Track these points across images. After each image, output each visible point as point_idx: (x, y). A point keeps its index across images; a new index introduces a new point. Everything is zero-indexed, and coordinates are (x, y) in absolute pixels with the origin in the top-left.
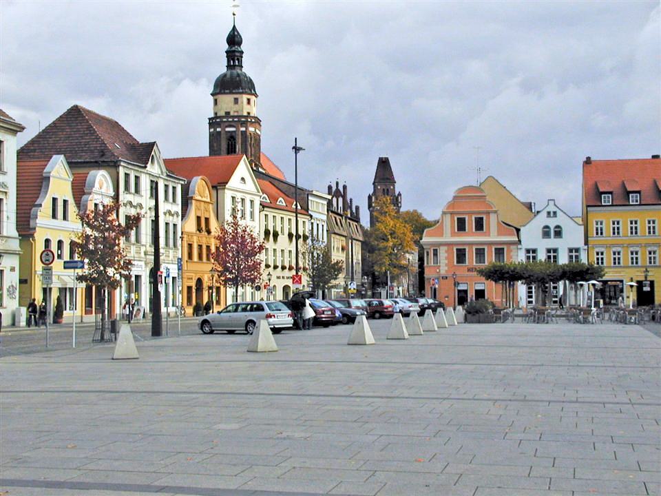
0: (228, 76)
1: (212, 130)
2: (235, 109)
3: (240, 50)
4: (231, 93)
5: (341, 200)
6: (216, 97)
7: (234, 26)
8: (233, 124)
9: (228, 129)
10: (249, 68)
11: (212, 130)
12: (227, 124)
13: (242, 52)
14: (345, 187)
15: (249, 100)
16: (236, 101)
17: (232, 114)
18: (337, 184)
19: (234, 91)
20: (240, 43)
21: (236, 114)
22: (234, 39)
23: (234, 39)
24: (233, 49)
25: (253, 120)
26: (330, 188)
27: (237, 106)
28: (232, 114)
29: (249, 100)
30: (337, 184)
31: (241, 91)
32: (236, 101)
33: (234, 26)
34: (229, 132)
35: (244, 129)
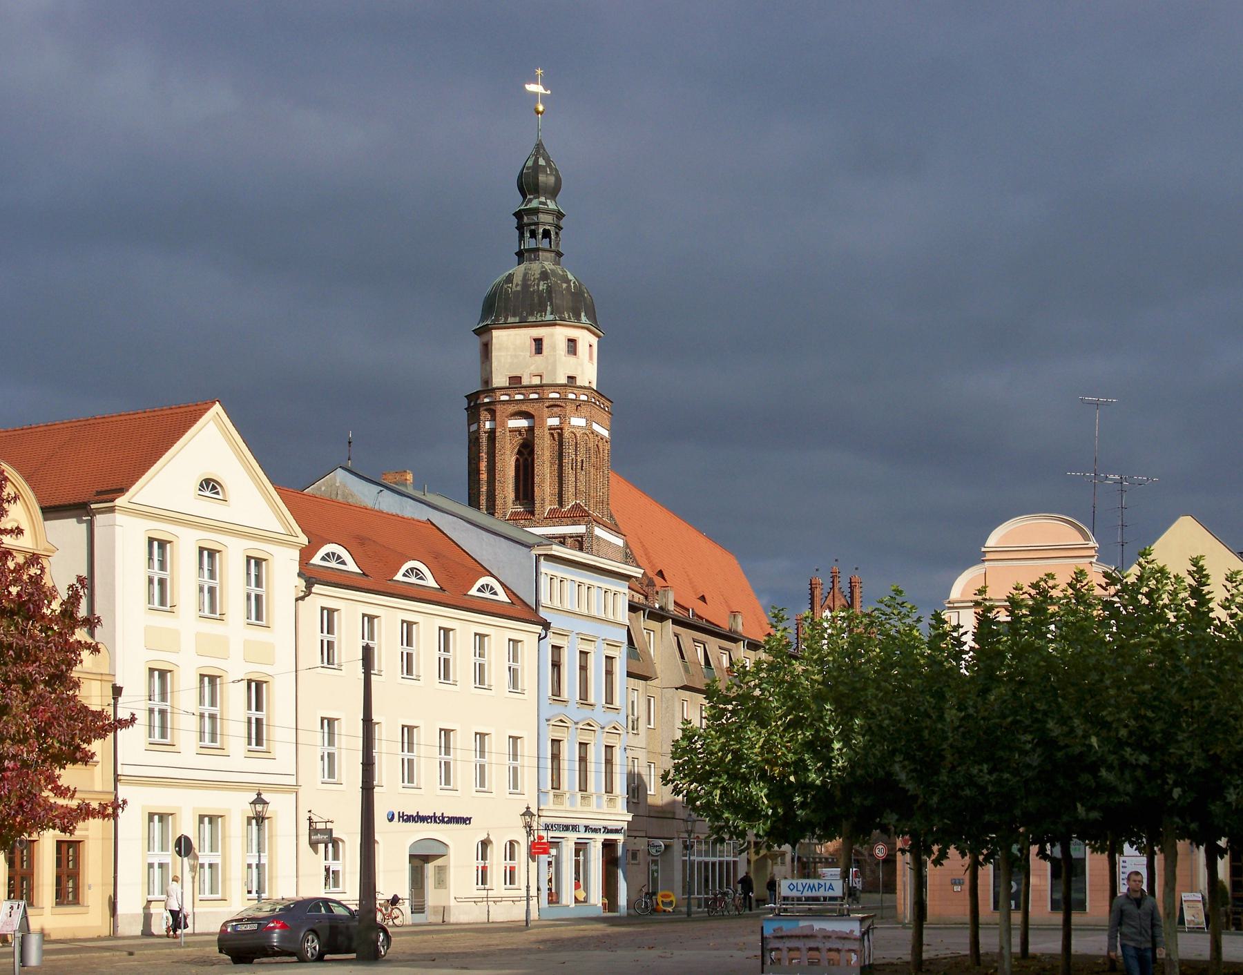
0: (518, 279)
2: (533, 369)
4: (523, 324)
6: (485, 338)
8: (524, 408)
11: (474, 428)
12: (512, 408)
15: (572, 343)
16: (538, 342)
17: (525, 382)
19: (531, 319)
21: (536, 381)
24: (534, 204)
25: (584, 398)
27: (538, 357)
28: (525, 382)
29: (572, 343)
31: (549, 317)
32: (538, 342)
34: (518, 431)
35: (554, 422)
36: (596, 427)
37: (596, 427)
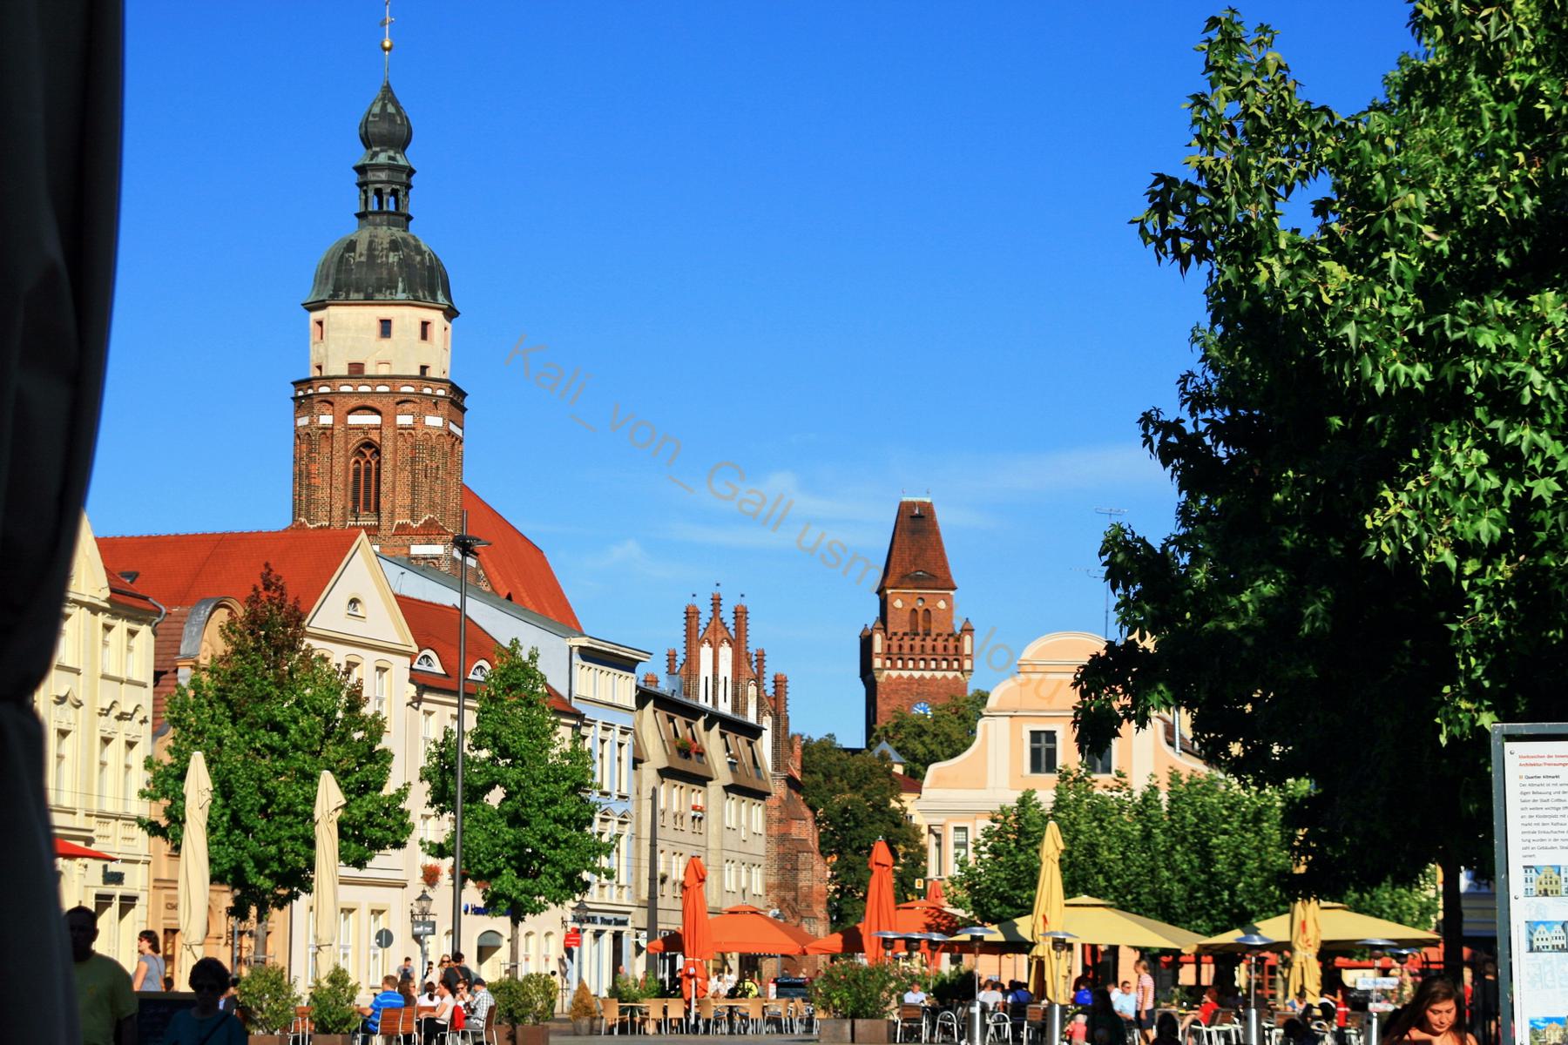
0: (362, 247)
1: (303, 421)
3: (401, 161)
5: (726, 652)
7: (388, 89)
8: (369, 403)
9: (353, 420)
10: (433, 225)
12: (354, 402)
13: (411, 172)
14: (740, 615)
16: (386, 327)
17: (369, 371)
18: (716, 602)
20: (401, 142)
21: (384, 370)
22: (387, 132)
23: (387, 132)
26: (691, 615)
27: (385, 342)
28: (369, 371)
30: (716, 602)
32: (386, 327)
33: (388, 89)
34: (359, 428)
35: (404, 420)
36: (453, 427)
37: (453, 427)
